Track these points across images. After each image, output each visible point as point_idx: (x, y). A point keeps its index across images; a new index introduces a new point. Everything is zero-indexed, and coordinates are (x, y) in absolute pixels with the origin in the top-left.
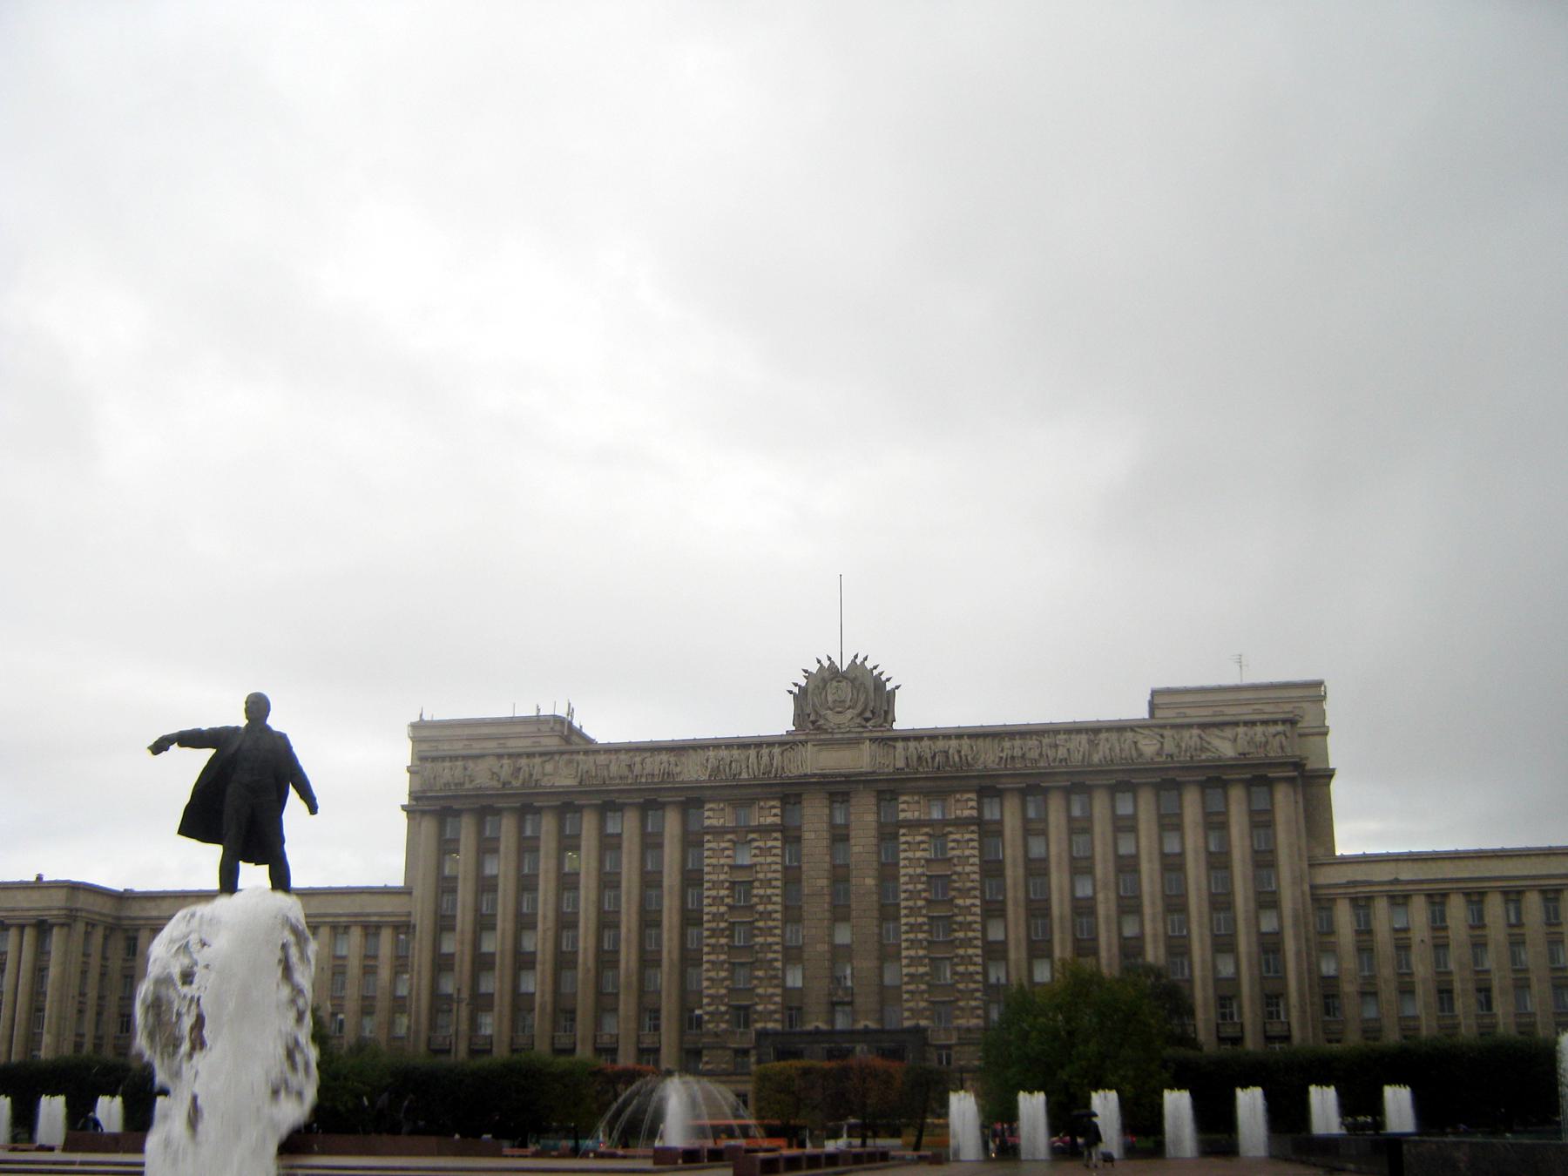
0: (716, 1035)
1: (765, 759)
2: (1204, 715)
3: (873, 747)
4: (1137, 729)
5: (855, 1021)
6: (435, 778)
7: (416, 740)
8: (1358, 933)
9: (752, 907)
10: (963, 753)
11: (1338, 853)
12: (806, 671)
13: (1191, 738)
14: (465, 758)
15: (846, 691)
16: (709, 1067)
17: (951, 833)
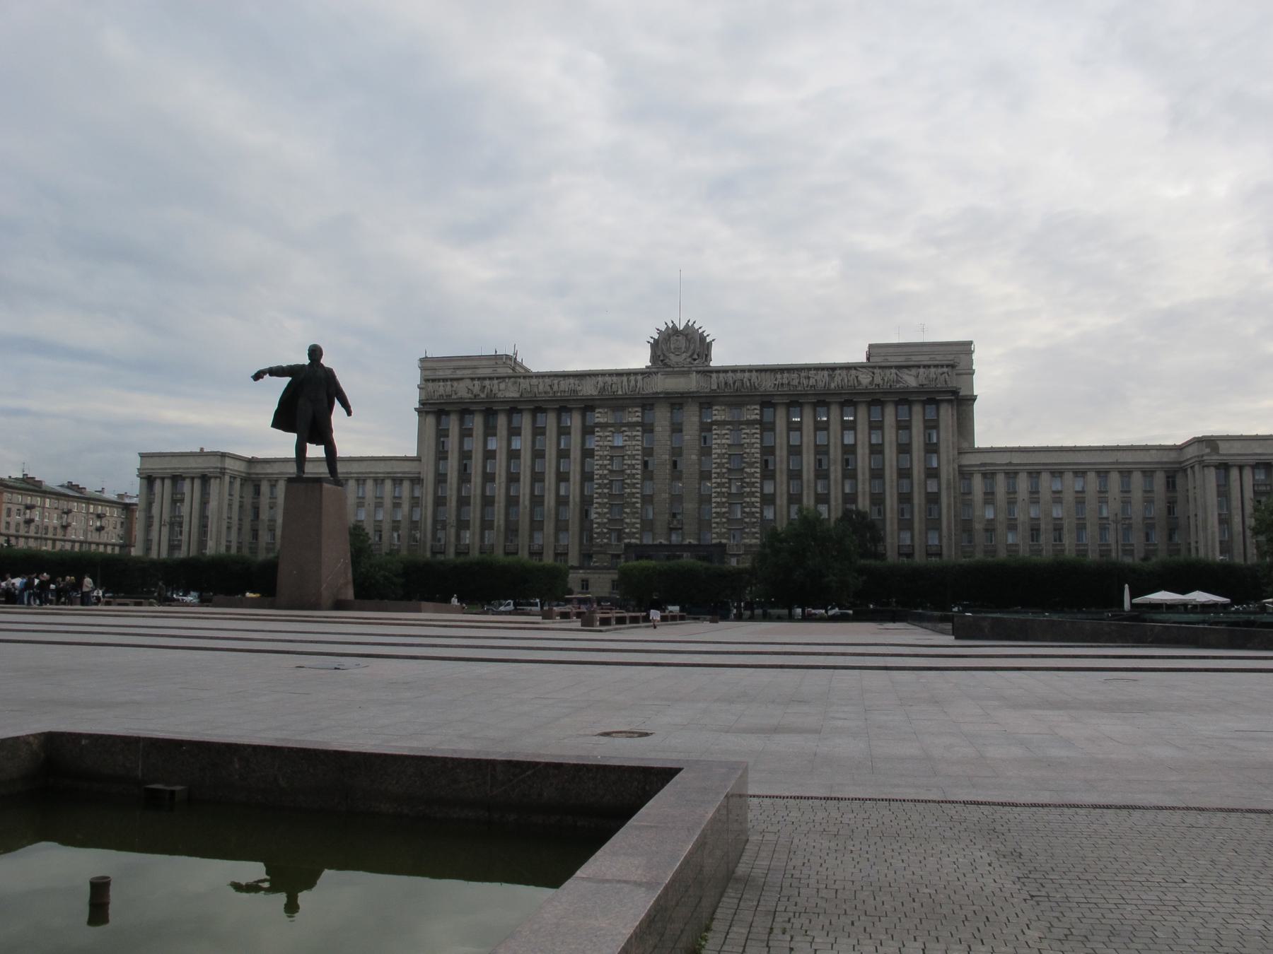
0: (601, 546)
1: (633, 383)
2: (899, 360)
3: (698, 376)
5: (683, 539)
6: (434, 392)
7: (423, 369)
8: (986, 494)
9: (623, 471)
10: (752, 381)
12: (658, 330)
13: (891, 374)
14: (452, 380)
15: (682, 342)
16: (596, 564)
17: (744, 429)
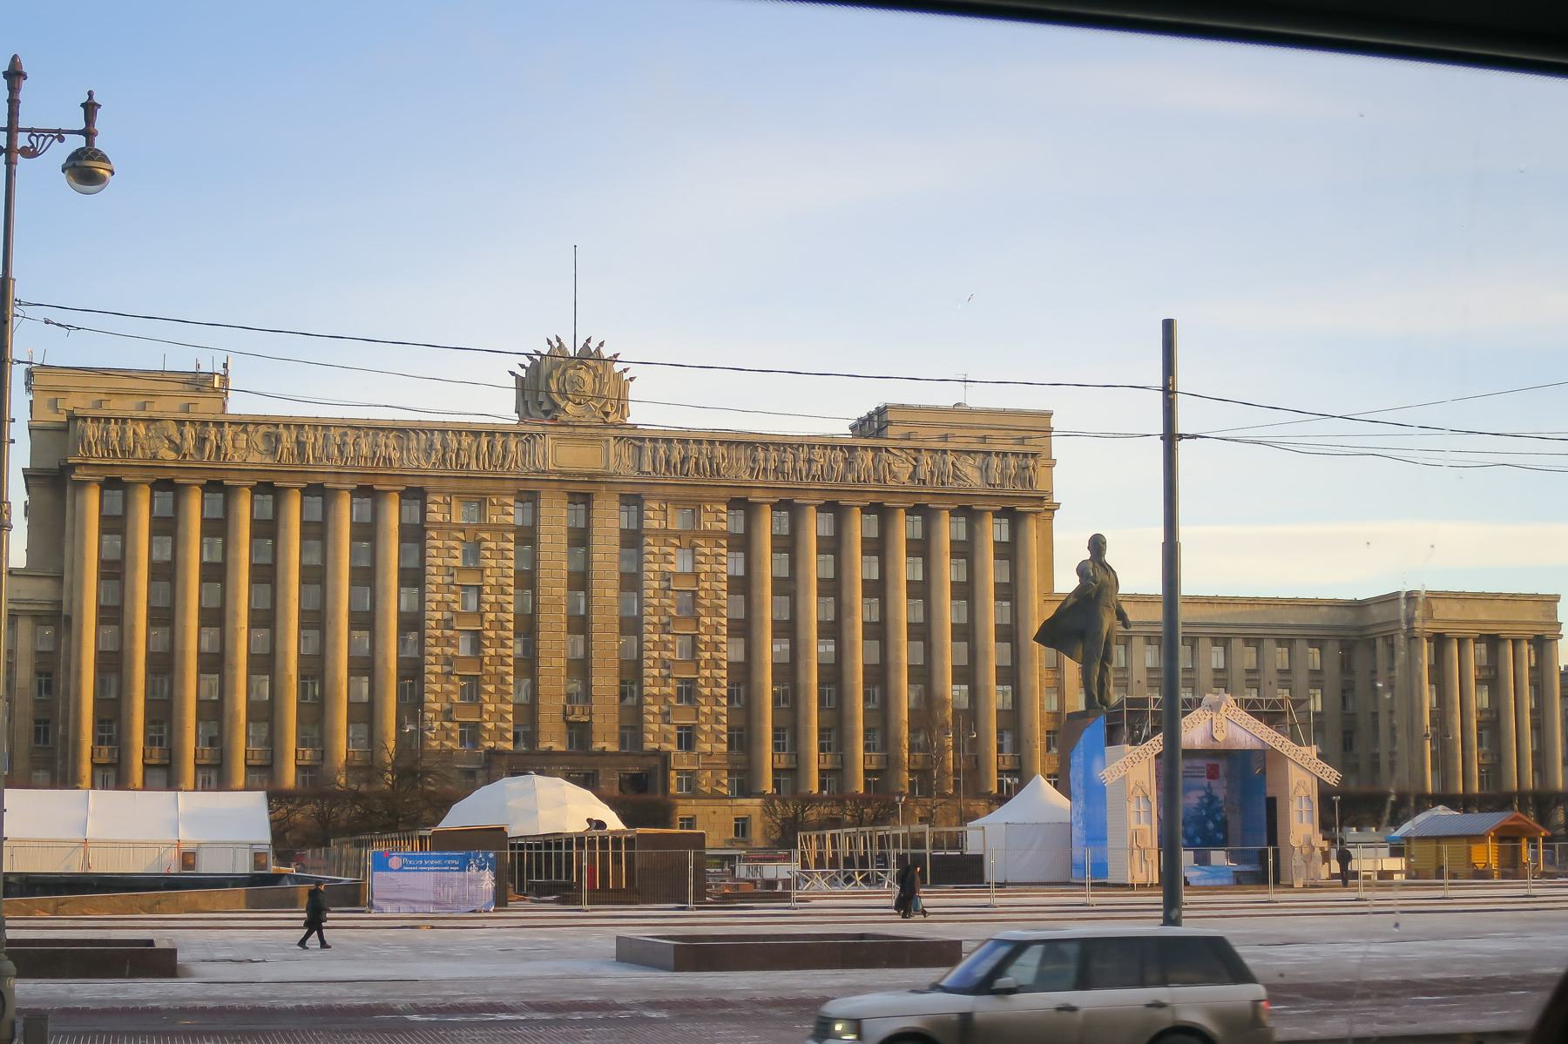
4: (891, 450)
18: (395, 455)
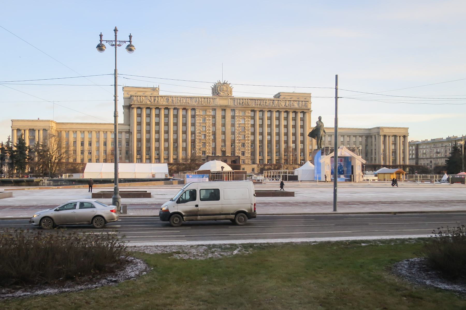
11: (311, 127)
18: (190, 102)
